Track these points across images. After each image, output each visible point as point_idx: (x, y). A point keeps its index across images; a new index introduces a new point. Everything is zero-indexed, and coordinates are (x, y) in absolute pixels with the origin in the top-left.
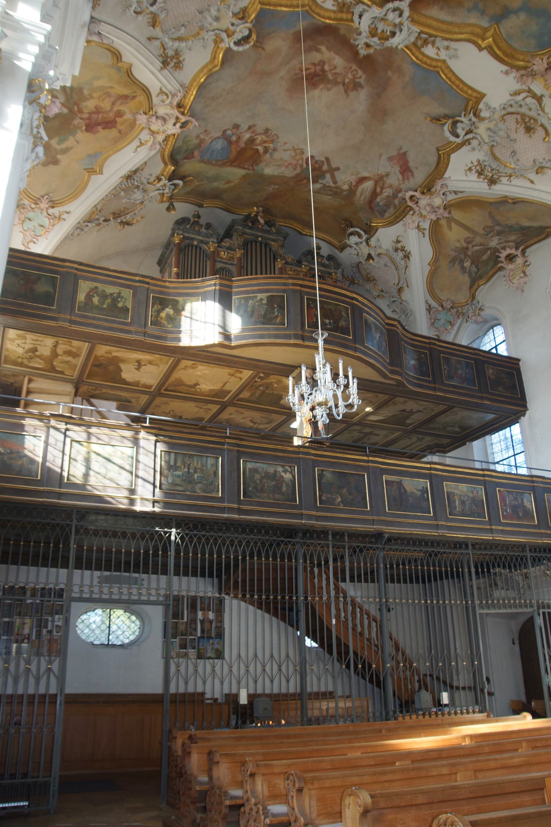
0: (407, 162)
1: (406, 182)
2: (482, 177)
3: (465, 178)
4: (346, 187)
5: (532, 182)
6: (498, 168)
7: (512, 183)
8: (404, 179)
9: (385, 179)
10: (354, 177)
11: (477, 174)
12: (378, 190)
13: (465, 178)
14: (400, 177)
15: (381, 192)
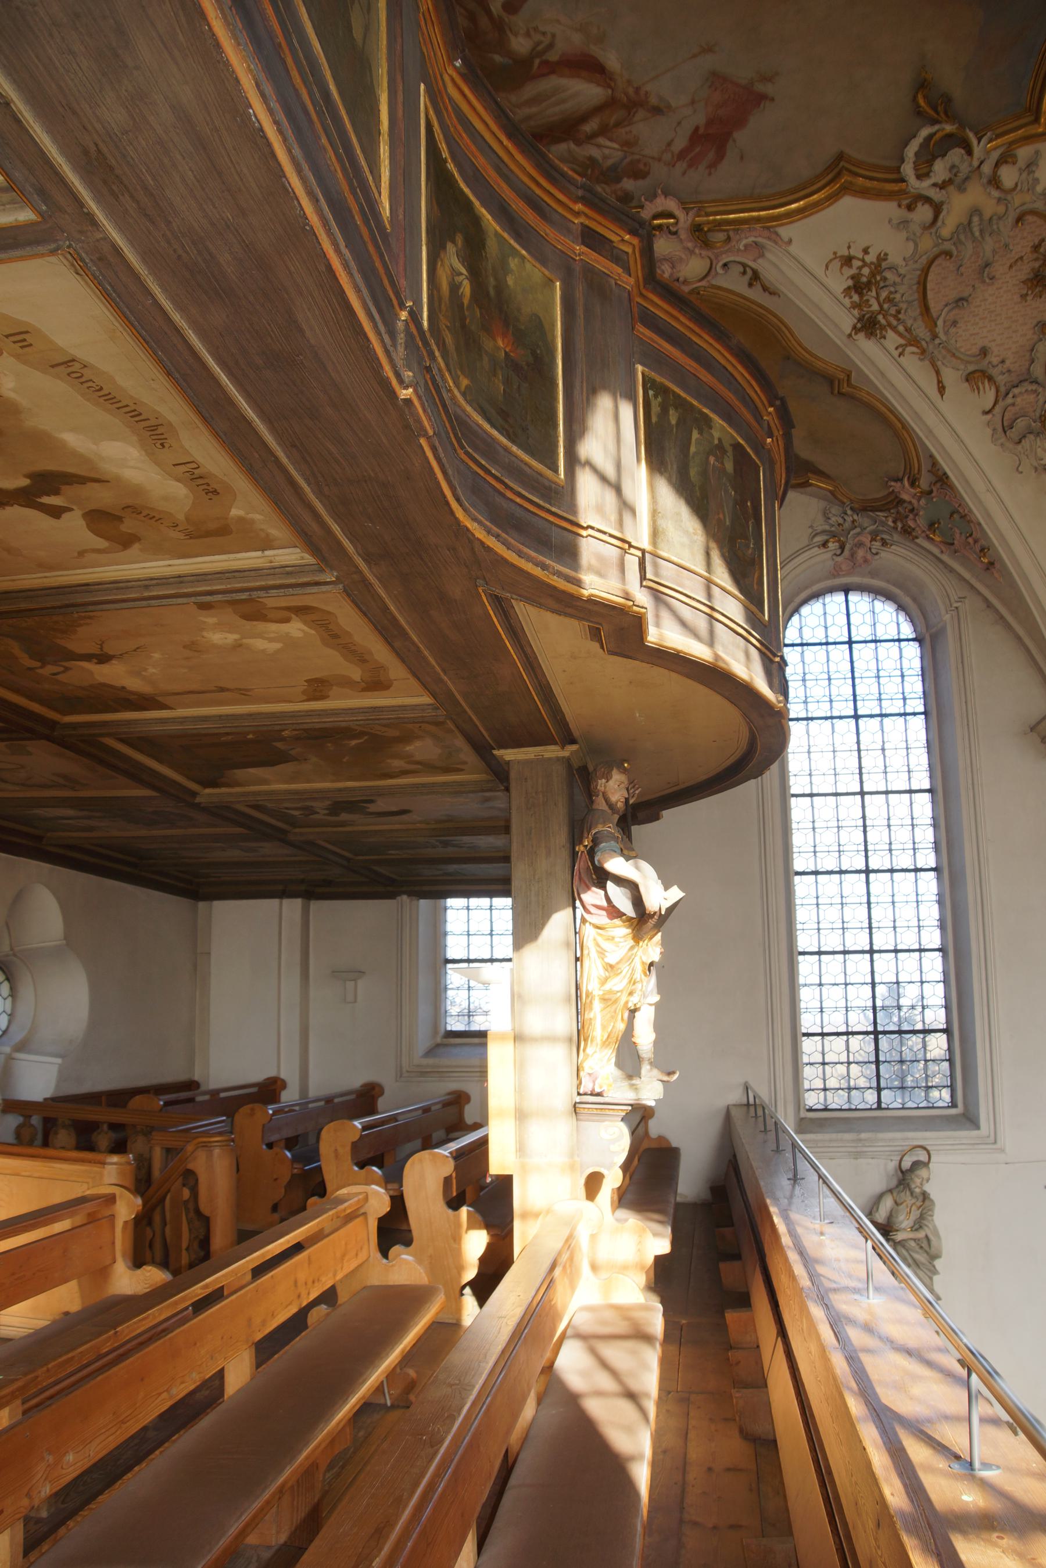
0: (739, 121)
1: (681, 166)
2: (856, 298)
3: (819, 271)
4: (520, 45)
5: (941, 389)
6: (904, 306)
7: (902, 359)
8: (682, 155)
9: (641, 114)
10: (577, 38)
11: (850, 283)
12: (589, 127)
13: (819, 271)
14: (680, 144)
15: (591, 137)
